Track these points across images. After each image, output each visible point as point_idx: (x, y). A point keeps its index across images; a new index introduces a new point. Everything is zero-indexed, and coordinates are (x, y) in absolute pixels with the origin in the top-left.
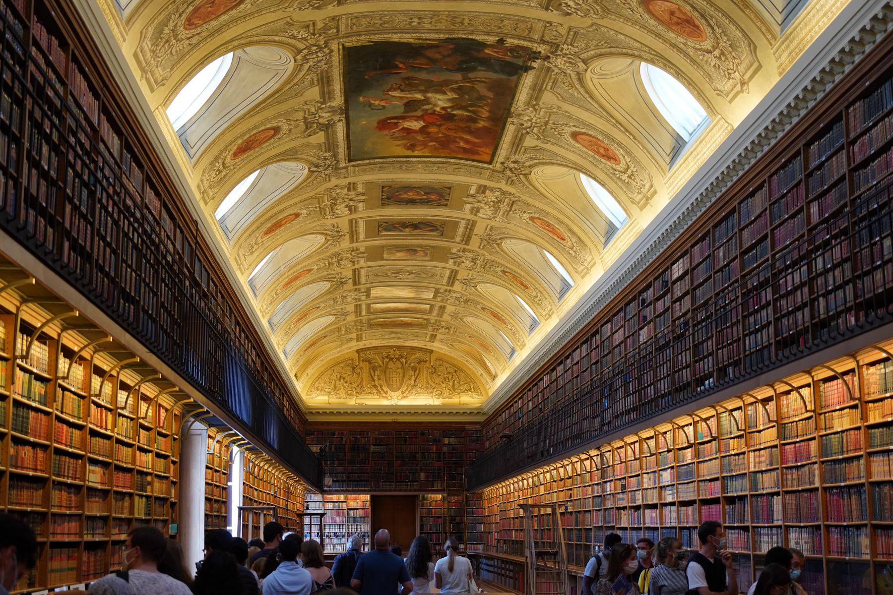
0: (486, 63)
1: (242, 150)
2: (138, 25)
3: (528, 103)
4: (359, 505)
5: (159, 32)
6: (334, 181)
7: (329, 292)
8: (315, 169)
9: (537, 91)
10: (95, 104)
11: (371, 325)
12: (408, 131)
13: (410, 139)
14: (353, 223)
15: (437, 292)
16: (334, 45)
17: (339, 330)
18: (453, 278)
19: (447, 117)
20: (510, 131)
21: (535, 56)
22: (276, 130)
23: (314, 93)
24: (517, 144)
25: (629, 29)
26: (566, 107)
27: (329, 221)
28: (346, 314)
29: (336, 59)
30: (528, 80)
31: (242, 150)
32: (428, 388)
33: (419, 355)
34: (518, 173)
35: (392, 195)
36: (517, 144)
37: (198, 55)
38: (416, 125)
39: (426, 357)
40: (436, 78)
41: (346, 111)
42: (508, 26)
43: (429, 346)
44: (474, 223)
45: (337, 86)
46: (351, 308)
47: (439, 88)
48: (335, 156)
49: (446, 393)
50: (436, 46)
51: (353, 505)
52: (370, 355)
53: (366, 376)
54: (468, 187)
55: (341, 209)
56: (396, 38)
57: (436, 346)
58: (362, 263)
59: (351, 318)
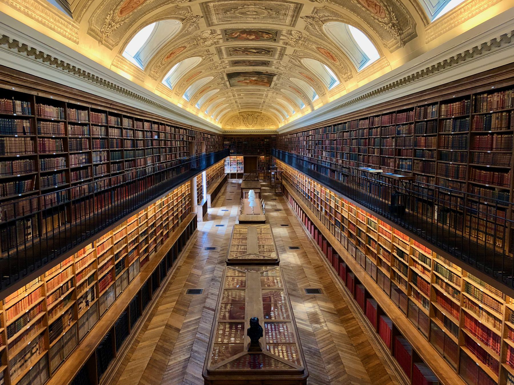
0: (264, 74)
4: (240, 159)
8: (221, 89)
9: (278, 79)
20: (273, 83)
30: (275, 78)
32: (260, 124)
33: (258, 114)
36: (276, 85)
49: (266, 125)
51: (238, 159)
52: (243, 114)
53: (242, 122)
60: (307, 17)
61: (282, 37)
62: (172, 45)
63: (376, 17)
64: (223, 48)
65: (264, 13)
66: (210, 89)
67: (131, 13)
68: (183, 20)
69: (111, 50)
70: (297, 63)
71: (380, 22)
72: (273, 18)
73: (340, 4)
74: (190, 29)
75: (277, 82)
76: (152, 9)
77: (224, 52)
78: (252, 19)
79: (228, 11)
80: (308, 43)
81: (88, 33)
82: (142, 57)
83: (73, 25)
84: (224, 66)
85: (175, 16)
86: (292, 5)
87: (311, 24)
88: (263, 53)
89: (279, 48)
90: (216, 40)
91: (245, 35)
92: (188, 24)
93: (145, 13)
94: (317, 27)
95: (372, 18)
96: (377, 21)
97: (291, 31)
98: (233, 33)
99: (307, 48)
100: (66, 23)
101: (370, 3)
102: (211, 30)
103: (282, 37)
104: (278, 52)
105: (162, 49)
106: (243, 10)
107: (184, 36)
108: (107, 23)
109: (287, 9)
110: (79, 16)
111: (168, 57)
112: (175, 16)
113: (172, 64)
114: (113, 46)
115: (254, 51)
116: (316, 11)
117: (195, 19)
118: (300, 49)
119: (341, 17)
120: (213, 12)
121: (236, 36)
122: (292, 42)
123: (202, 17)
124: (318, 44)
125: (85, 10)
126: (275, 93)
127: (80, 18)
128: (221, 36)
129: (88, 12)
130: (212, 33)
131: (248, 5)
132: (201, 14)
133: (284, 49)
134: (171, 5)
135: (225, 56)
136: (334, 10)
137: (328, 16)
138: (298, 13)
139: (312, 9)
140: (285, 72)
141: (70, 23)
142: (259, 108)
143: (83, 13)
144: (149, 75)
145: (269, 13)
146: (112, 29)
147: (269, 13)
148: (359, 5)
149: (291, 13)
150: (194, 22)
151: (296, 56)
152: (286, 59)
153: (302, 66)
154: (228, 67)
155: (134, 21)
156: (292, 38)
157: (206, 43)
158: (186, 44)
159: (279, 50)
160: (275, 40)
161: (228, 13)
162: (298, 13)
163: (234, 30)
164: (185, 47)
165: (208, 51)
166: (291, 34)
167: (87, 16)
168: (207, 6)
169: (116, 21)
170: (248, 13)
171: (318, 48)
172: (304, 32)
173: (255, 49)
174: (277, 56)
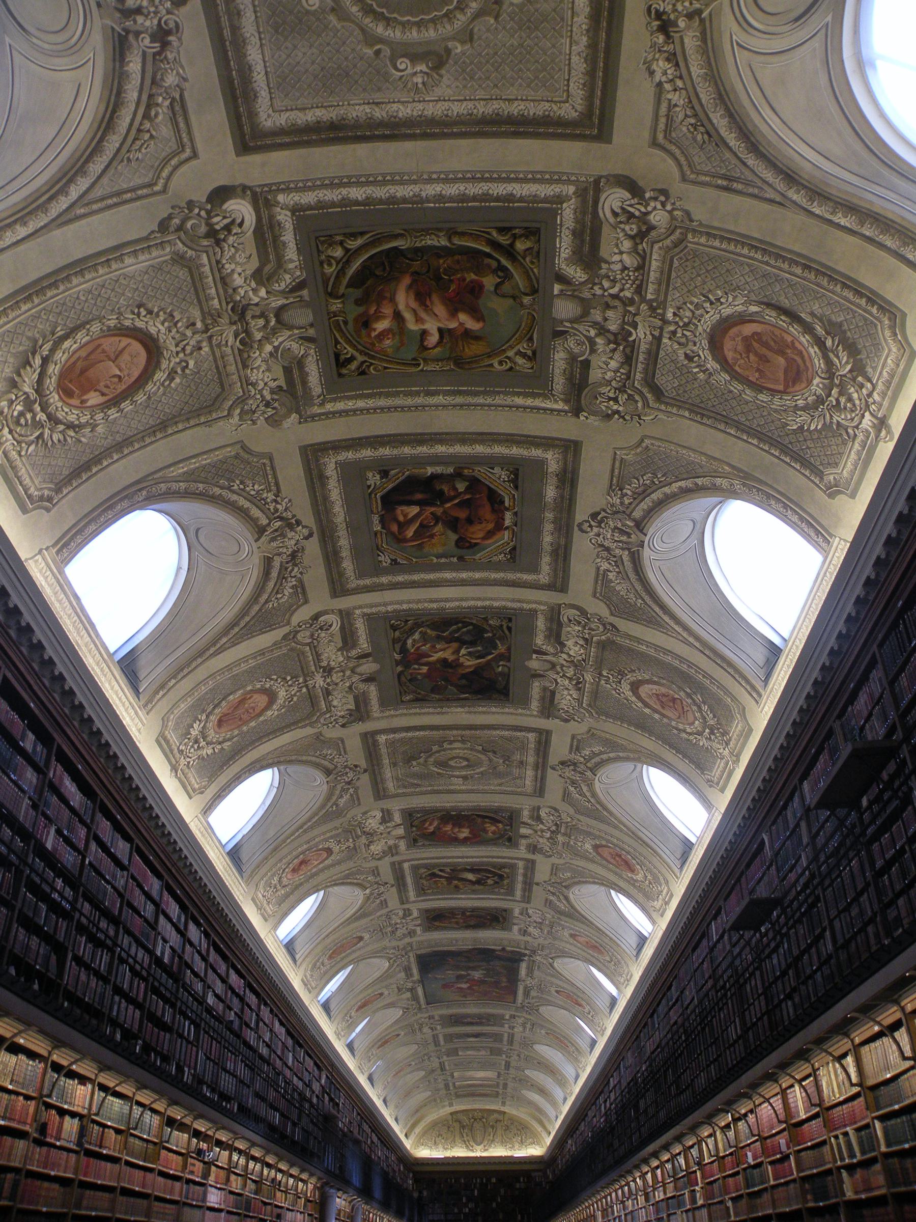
0: (499, 958)
1: (360, 1007)
2: (304, 966)
3: (527, 975)
5: (314, 965)
6: (419, 1015)
7: (425, 1077)
8: (406, 1010)
10: (283, 1030)
11: (458, 1096)
12: (461, 988)
13: (463, 993)
14: (435, 1037)
15: (499, 1074)
16: (411, 954)
17: (435, 1100)
18: (508, 1065)
19: (481, 982)
21: (525, 955)
22: (381, 994)
23: (402, 975)
24: (527, 993)
25: (568, 946)
26: (549, 978)
27: (419, 1036)
28: (438, 1090)
29: (412, 959)
30: (523, 966)
31: (360, 1007)
32: (503, 1143)
33: (496, 1115)
34: (533, 1009)
35: (457, 1020)
36: (527, 993)
37: (335, 969)
38: (464, 986)
39: (501, 1117)
40: (471, 965)
41: (422, 981)
42: (506, 943)
43: (502, 1109)
44: (513, 1035)
45: (415, 971)
46: (441, 1086)
47: (474, 968)
48: (419, 1003)
50: (470, 951)
54: (503, 1016)
55: (426, 1030)
56: (446, 949)
57: (505, 1109)
58: (445, 1058)
59: (443, 1092)
60: (563, 763)
61: (523, 831)
62: (306, 837)
63: (681, 726)
64: (406, 866)
65: (480, 763)
66: (381, 1003)
67: (236, 732)
68: (328, 772)
69: (190, 798)
70: (562, 906)
71: (690, 734)
72: (499, 775)
73: (615, 718)
74: (342, 802)
75: (529, 982)
76: (274, 732)
77: (409, 880)
78: (460, 781)
79: (415, 759)
80: (576, 839)
81: (157, 741)
82: (244, 855)
83: (136, 713)
84: (411, 927)
85: (314, 759)
86: (532, 736)
87: (573, 783)
88: (490, 882)
89: (521, 864)
90: (391, 842)
91: (448, 828)
92: (339, 787)
93: (261, 738)
94: (585, 789)
95: (675, 731)
96: (684, 735)
97: (539, 808)
98: (425, 821)
99: (577, 854)
100: (127, 704)
101: (664, 699)
102: (382, 811)
103: (523, 831)
104: (520, 878)
105: (284, 841)
106: (442, 756)
107: (328, 817)
108: (193, 737)
109: (523, 747)
110: (149, 701)
111: (294, 870)
112: (314, 759)
113: (302, 890)
114: (194, 790)
115: (470, 876)
116: (576, 745)
117: (351, 775)
118: (562, 861)
119: (624, 749)
120: (386, 761)
121: (432, 829)
122: (543, 843)
123: (365, 771)
124: (595, 837)
125: (161, 693)
126: (528, 1026)
127: (150, 706)
128: (401, 831)
129: (165, 699)
130: (384, 821)
131: (451, 742)
132: (363, 764)
133: (531, 866)
134: (309, 731)
135: (412, 894)
136: (608, 736)
137: (601, 753)
138: (544, 758)
139: (569, 740)
140: (541, 941)
141: (133, 707)
142: (497, 1095)
143: (158, 697)
144: (253, 899)
145: (490, 760)
146: (199, 753)
147: (490, 760)
148: (647, 711)
149: (531, 759)
150: (349, 783)
151: (561, 887)
152: (538, 893)
153: (574, 914)
154: (419, 932)
155: (240, 751)
156: (542, 831)
157: (372, 847)
158: (332, 844)
159: (521, 871)
160: (510, 840)
161: (414, 763)
162: (544, 758)
163: (428, 813)
164: (329, 851)
165: (375, 872)
166: (539, 819)
167: (163, 706)
168: (375, 743)
169: (209, 739)
170: (452, 763)
171: (596, 847)
172: (564, 807)
173: (472, 870)
174: (518, 893)
